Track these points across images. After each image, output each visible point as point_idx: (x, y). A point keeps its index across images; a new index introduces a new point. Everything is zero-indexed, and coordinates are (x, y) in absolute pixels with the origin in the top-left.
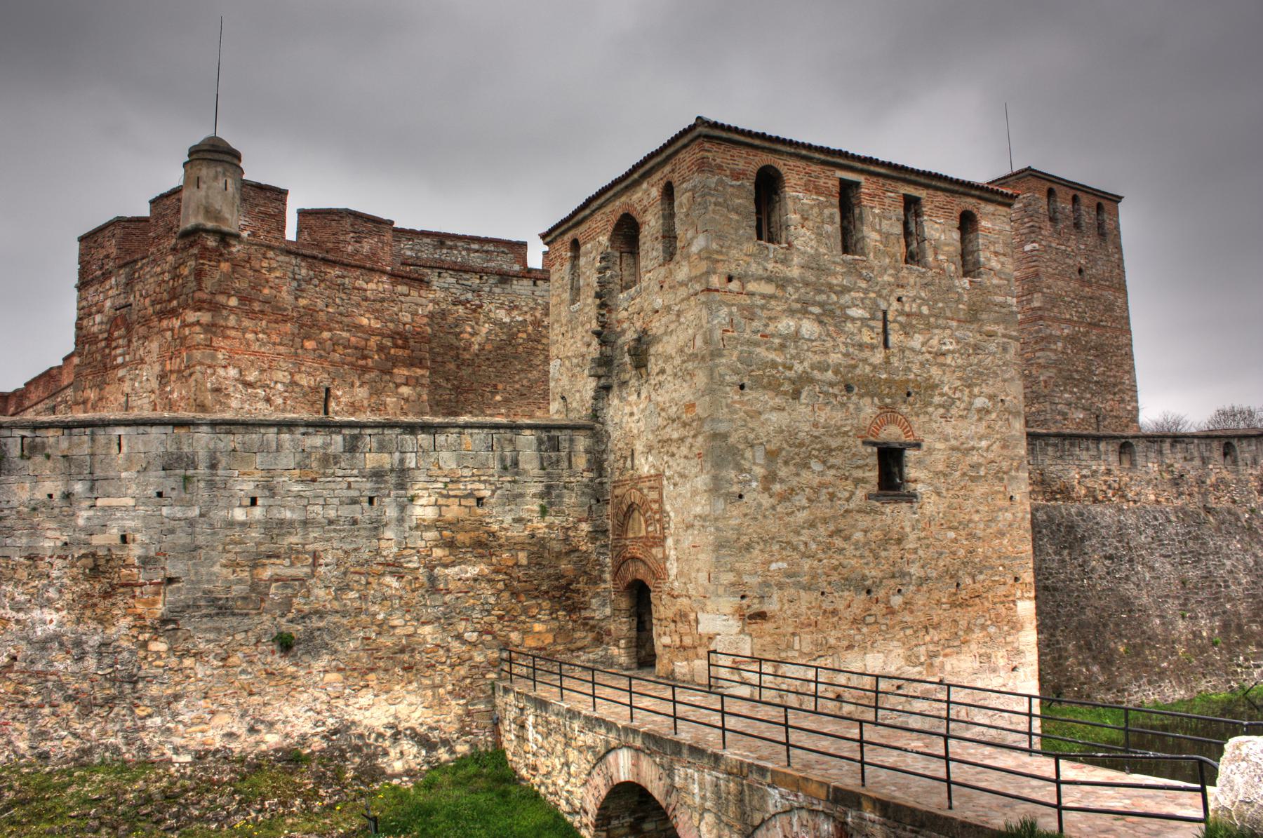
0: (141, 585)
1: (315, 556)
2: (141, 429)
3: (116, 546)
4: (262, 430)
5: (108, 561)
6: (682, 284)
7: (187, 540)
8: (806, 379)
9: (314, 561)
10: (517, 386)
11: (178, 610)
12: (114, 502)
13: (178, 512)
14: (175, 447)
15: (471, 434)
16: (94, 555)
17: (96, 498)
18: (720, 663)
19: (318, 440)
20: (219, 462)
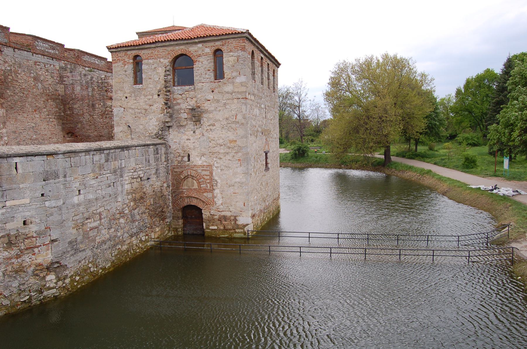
0: (38, 247)
1: (100, 214)
2: (29, 158)
3: (21, 227)
4: (80, 155)
5: (16, 237)
6: (228, 93)
7: (59, 218)
8: (258, 131)
9: (100, 217)
10: (9, 103)
11: (60, 256)
12: (16, 202)
13: (53, 203)
14: (49, 167)
15: (138, 149)
16: (8, 235)
17: (5, 202)
18: (283, 235)
19: (97, 158)
20: (67, 173)
